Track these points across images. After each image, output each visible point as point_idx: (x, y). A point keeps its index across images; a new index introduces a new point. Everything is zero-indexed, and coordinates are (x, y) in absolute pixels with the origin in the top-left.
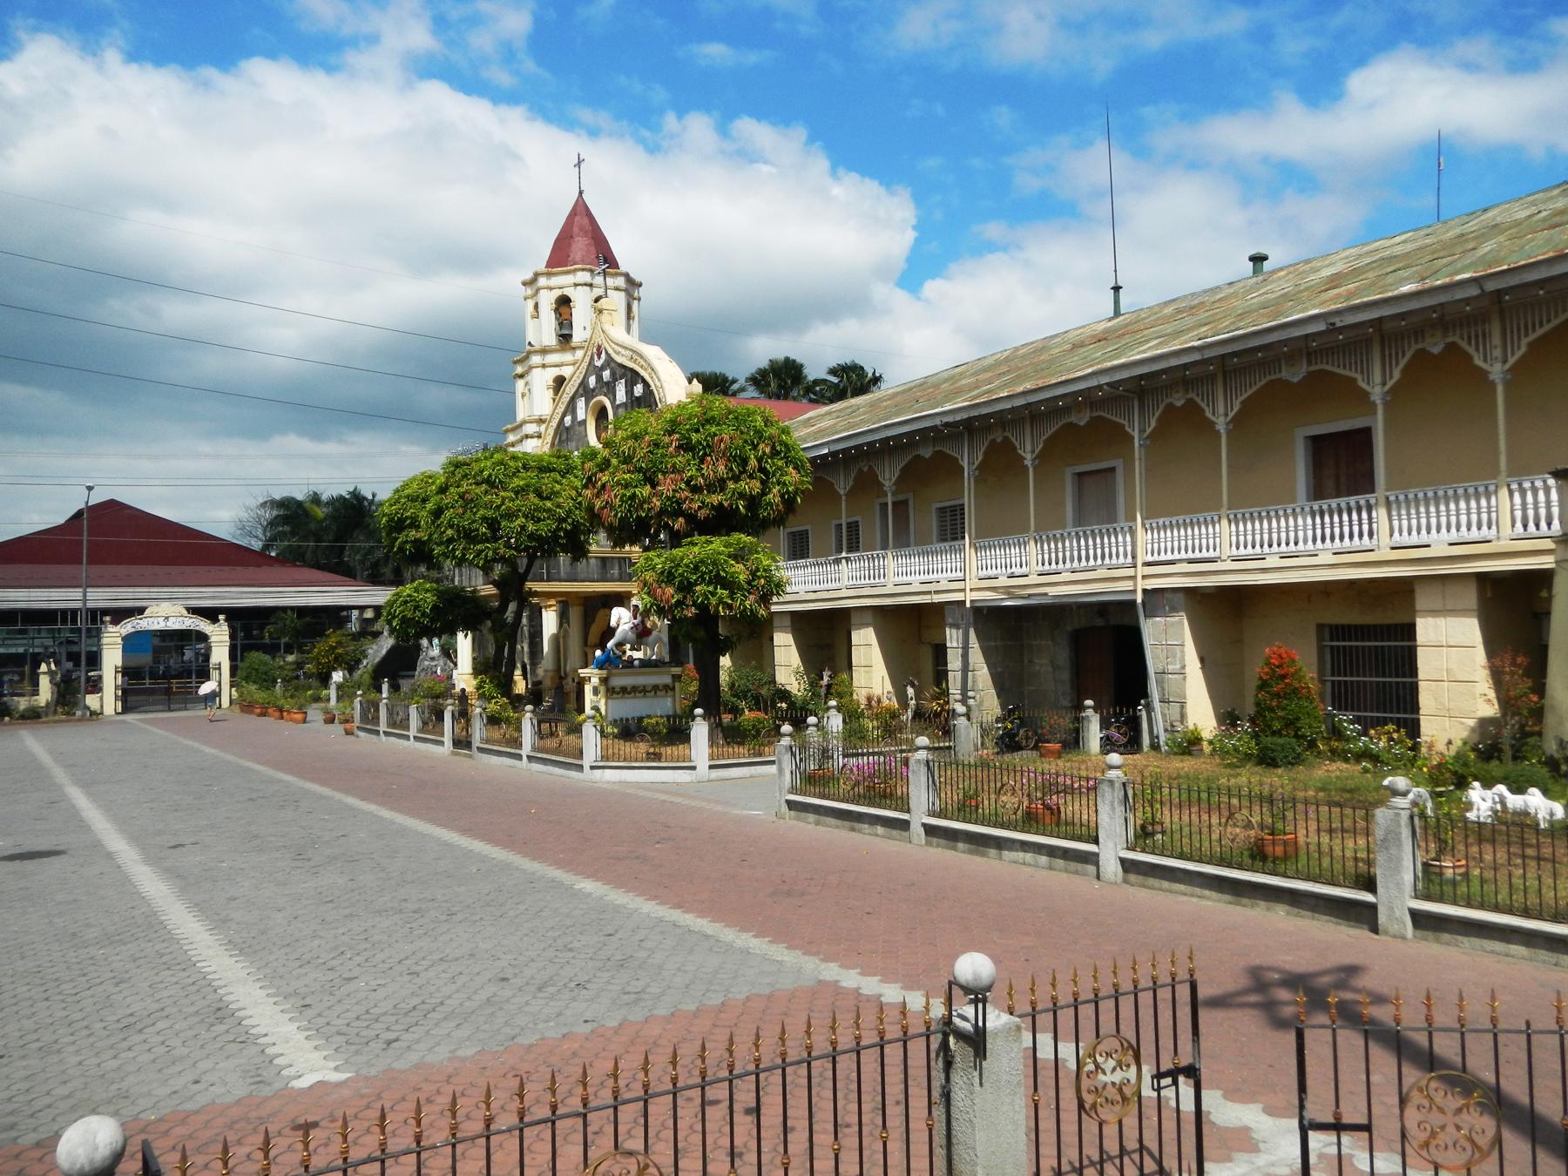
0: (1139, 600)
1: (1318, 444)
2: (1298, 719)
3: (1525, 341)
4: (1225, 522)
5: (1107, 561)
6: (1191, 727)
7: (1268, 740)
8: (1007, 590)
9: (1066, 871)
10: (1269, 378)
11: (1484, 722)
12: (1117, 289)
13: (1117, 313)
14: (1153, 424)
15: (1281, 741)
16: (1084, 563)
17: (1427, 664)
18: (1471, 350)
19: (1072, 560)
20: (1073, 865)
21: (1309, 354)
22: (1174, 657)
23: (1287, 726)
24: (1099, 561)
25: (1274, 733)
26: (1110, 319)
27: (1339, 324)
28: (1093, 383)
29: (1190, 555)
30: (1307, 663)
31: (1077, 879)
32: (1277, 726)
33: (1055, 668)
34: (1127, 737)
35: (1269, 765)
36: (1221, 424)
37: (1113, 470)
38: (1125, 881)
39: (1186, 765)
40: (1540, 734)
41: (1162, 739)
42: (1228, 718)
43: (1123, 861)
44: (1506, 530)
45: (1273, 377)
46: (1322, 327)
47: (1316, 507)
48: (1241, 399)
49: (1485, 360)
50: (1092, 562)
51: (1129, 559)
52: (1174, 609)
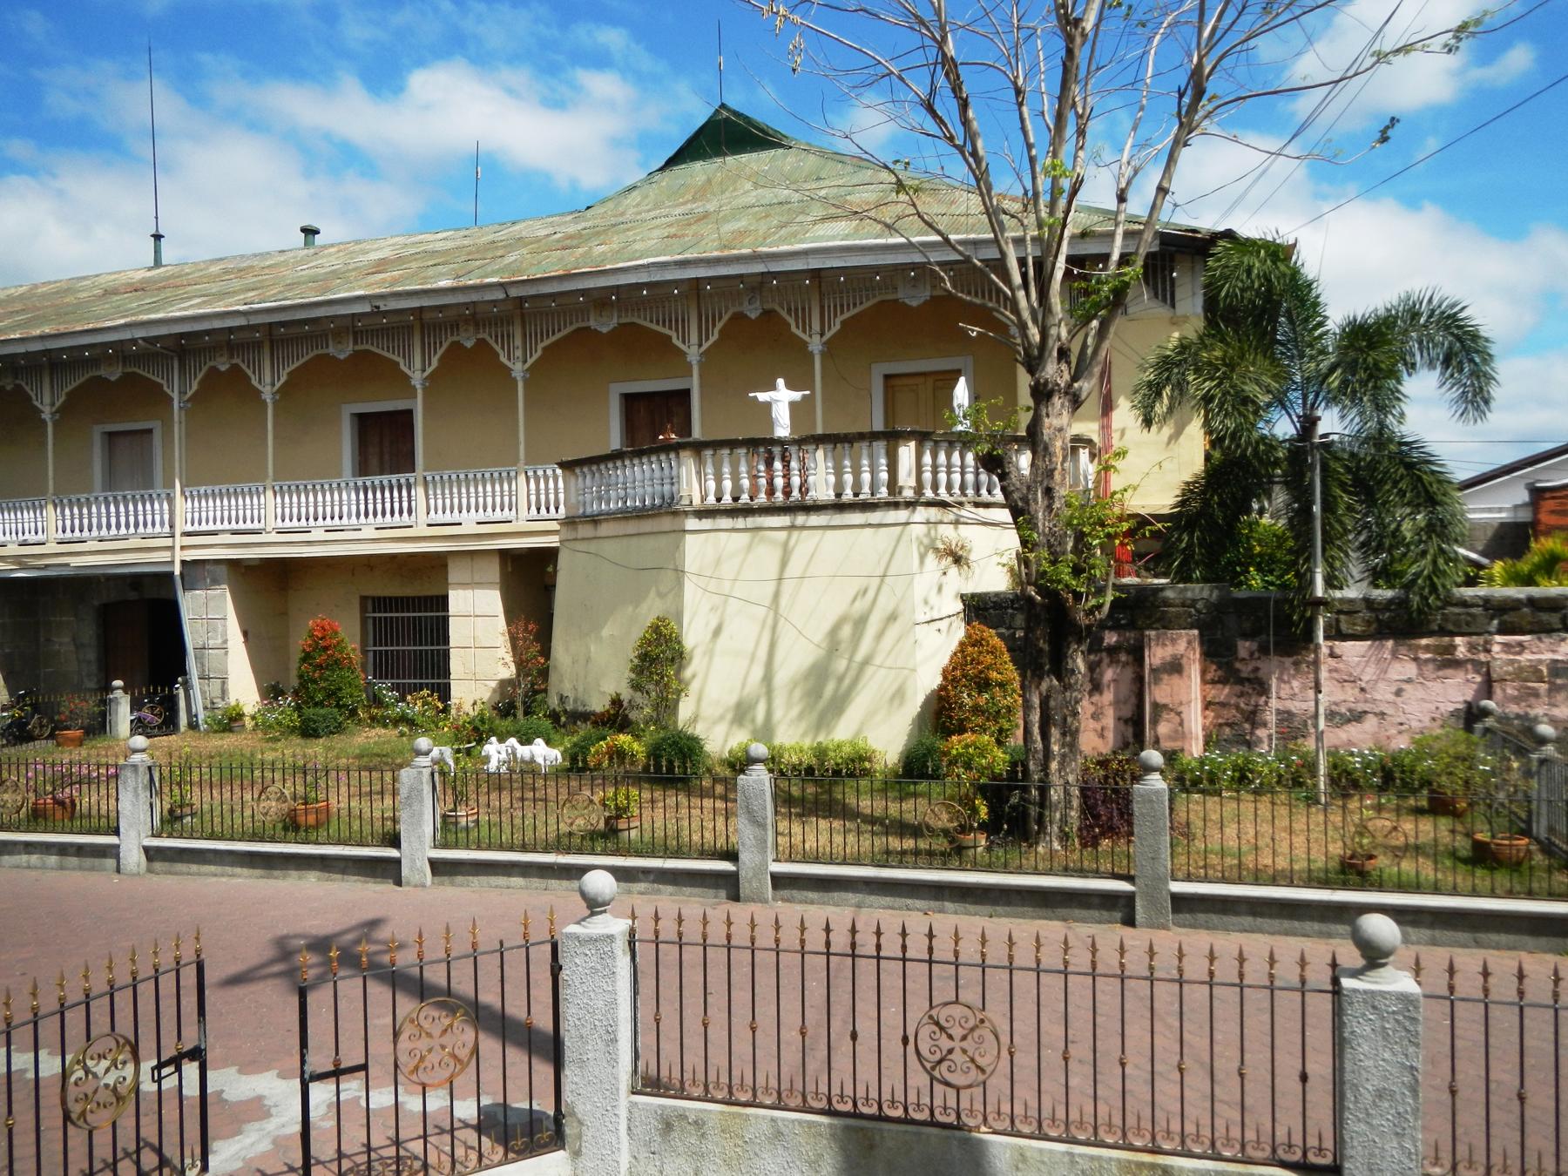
0: (177, 572)
1: (364, 423)
2: (340, 689)
3: (541, 346)
4: (270, 493)
5: (141, 529)
6: (233, 703)
7: (309, 712)
8: (18, 559)
9: (81, 868)
10: (316, 352)
11: (503, 684)
12: (158, 237)
13: (158, 263)
14: (195, 387)
15: (322, 711)
16: (114, 531)
17: (458, 632)
18: (498, 348)
19: (99, 527)
20: (88, 862)
21: (355, 333)
22: (215, 630)
23: (329, 696)
24: (132, 530)
25: (316, 704)
26: (150, 269)
28: (126, 335)
29: (234, 526)
30: (349, 635)
31: (93, 877)
32: (319, 697)
33: (79, 646)
34: (161, 715)
36: (267, 393)
37: (150, 431)
38: (149, 871)
39: (227, 742)
40: (545, 691)
41: (201, 717)
42: (271, 692)
43: (147, 850)
45: (320, 352)
46: (368, 309)
47: (360, 483)
48: (288, 370)
50: (123, 531)
51: (167, 528)
52: (216, 581)
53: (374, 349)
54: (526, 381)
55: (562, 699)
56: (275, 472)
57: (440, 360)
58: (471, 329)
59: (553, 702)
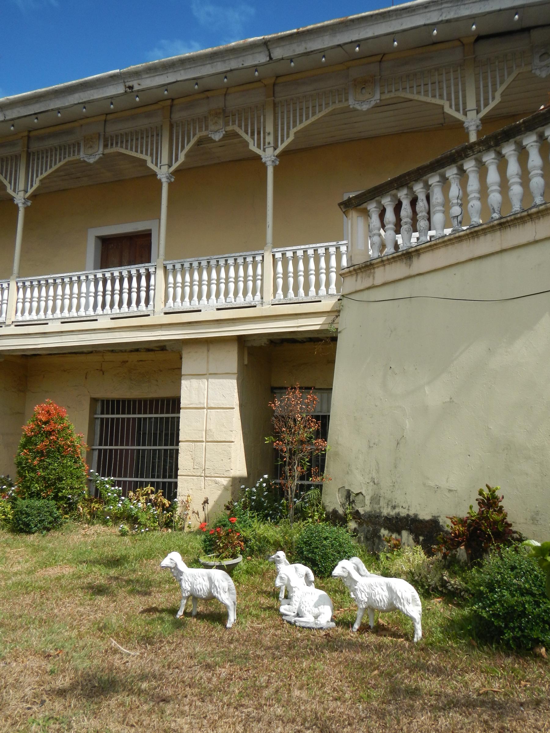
1: (106, 243)
2: (60, 479)
3: (293, 131)
11: (236, 481)
15: (38, 503)
17: (189, 425)
21: (106, 140)
25: (31, 496)
27: (136, 88)
30: (77, 429)
32: (36, 487)
35: (21, 531)
36: (19, 199)
40: (320, 487)
44: (269, 297)
45: (72, 158)
47: (99, 275)
48: (40, 177)
49: (259, 146)
53: (123, 151)
54: (276, 169)
55: (349, 497)
56: (20, 267)
57: (187, 156)
58: (221, 122)
59: (333, 501)
